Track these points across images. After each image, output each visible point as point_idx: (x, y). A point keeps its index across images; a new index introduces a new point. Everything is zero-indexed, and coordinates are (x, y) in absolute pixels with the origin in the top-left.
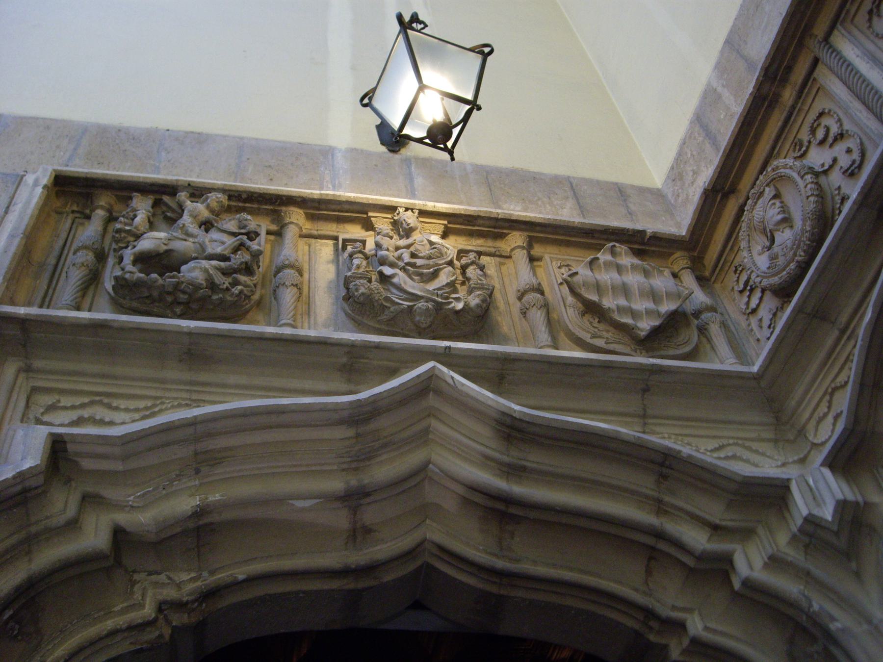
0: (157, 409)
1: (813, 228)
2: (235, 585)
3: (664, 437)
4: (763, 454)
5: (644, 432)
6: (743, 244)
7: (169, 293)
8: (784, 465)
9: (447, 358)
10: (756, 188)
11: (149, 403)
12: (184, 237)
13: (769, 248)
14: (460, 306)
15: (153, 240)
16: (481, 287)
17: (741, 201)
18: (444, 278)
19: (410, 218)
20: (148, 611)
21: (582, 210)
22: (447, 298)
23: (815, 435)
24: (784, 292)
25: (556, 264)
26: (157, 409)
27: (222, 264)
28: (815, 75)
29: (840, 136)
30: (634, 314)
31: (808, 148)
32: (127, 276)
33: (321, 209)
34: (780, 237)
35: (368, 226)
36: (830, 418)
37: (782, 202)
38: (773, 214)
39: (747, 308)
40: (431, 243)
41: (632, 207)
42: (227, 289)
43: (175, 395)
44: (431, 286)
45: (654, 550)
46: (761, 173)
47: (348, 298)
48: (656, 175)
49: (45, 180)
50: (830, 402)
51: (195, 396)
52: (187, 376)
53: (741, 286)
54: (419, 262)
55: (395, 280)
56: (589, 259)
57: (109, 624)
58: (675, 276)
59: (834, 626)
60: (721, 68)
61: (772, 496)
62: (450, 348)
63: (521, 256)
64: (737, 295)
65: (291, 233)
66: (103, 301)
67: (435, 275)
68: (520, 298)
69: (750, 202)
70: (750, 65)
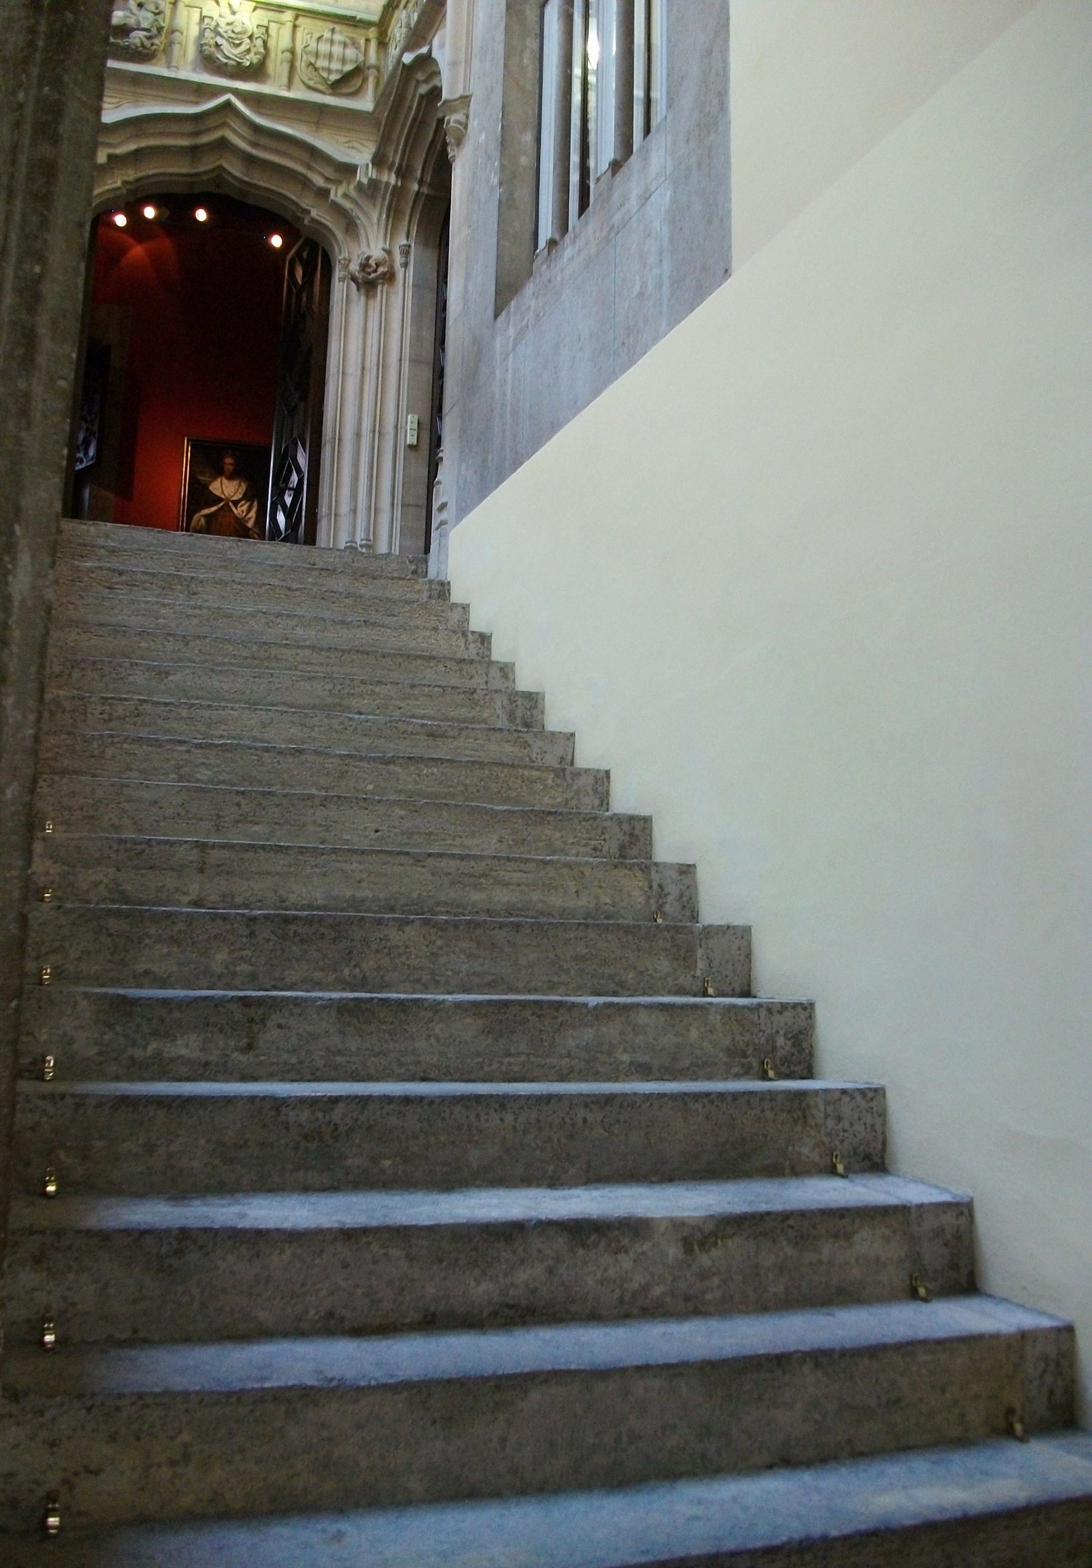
2: (148, 177)
9: (236, 92)
14: (248, 64)
18: (243, 47)
20: (119, 184)
30: (329, 71)
44: (237, 51)
45: (306, 184)
52: (132, 89)
57: (107, 187)
59: (358, 222)
61: (349, 170)
67: (240, 44)
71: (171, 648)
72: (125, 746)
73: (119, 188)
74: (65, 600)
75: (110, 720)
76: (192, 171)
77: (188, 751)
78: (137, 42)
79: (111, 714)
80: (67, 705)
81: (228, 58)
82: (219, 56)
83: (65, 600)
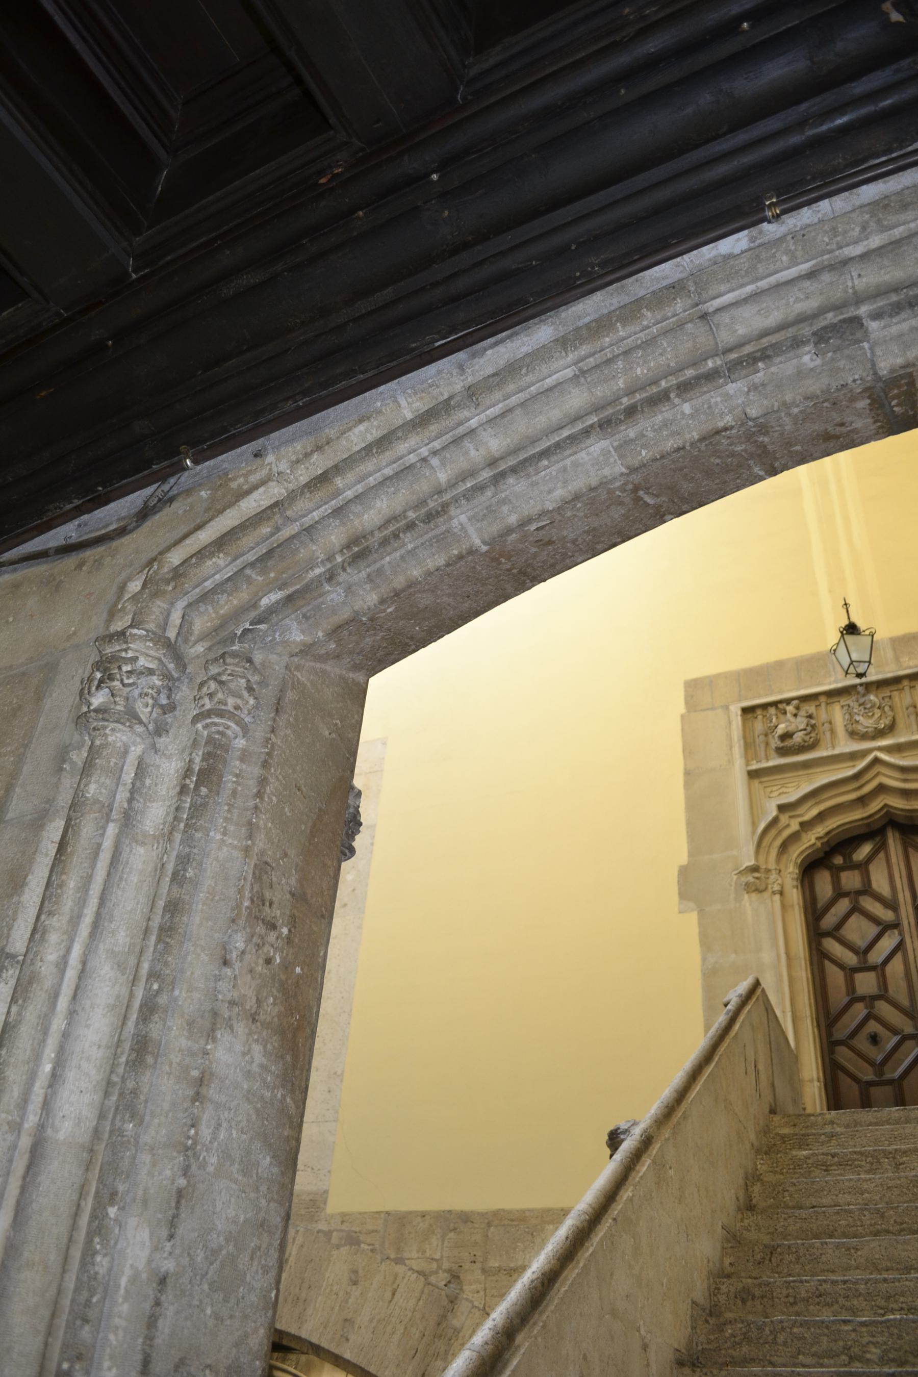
9: (880, 749)
15: (782, 728)
49: (739, 712)
57: (805, 846)
66: (773, 753)
67: (873, 715)
68: (907, 709)
71: (868, 1222)
72: (795, 1330)
73: (814, 844)
74: (781, 1188)
75: (795, 1303)
77: (854, 1330)
79: (795, 1297)
80: (757, 1293)
81: (868, 727)
82: (860, 728)
83: (781, 1188)
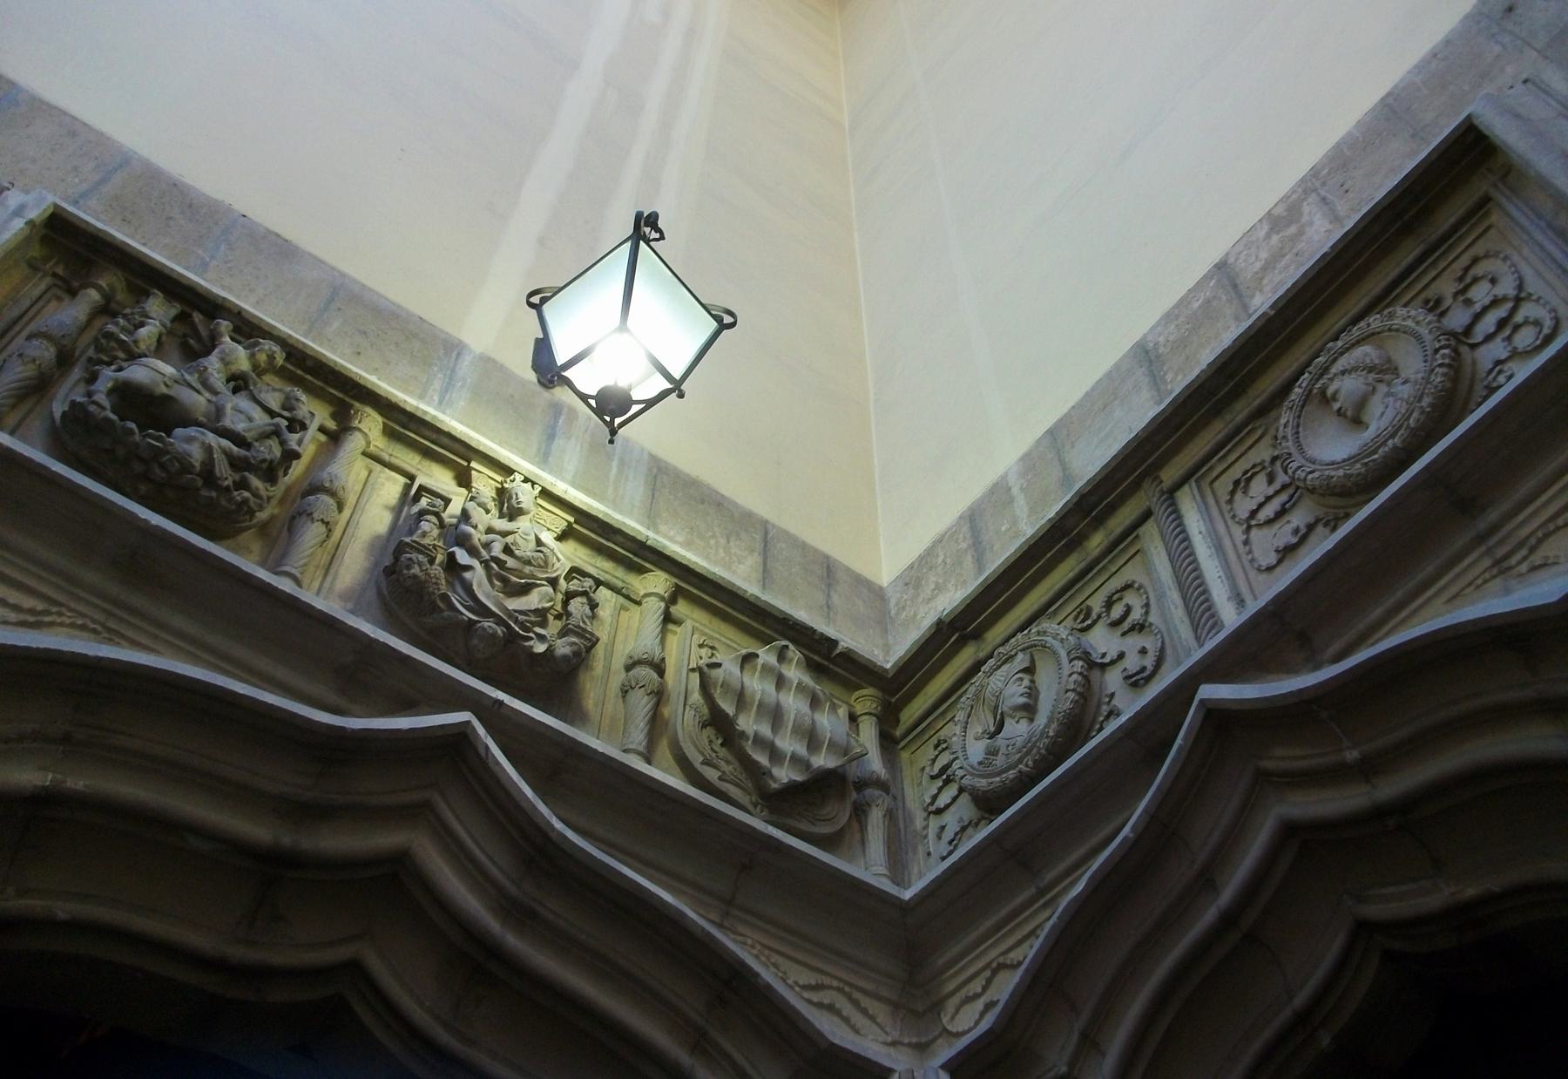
0: (47, 619)
1: (1058, 735)
3: (744, 947)
4: (872, 1018)
5: (720, 926)
6: (960, 716)
7: (141, 459)
8: (894, 1044)
9: (491, 714)
10: (1008, 647)
11: (40, 606)
12: (199, 386)
13: (992, 736)
14: (540, 648)
16: (581, 632)
17: (982, 655)
18: (533, 600)
19: (525, 495)
21: (766, 577)
22: (527, 630)
23: (953, 1018)
24: (988, 804)
25: (697, 639)
26: (47, 619)
27: (235, 449)
28: (1141, 530)
29: (1140, 627)
30: (775, 755)
31: (1095, 622)
32: (92, 408)
33: (407, 427)
34: (1009, 725)
35: (464, 479)
36: (979, 1005)
37: (1032, 681)
38: (1015, 693)
39: (932, 803)
40: (539, 542)
41: (835, 598)
42: (227, 489)
43: (81, 608)
44: (513, 604)
46: (1022, 629)
47: (390, 571)
48: (886, 570)
50: (989, 981)
51: (112, 624)
53: (936, 770)
54: (511, 562)
55: (467, 575)
56: (744, 651)
58: (853, 718)
60: (1029, 462)
62: (501, 703)
63: (654, 608)
64: (925, 779)
65: (354, 443)
67: (525, 590)
68: (628, 668)
69: (991, 662)
70: (1067, 479)
76: (237, 953)
78: (196, 454)
